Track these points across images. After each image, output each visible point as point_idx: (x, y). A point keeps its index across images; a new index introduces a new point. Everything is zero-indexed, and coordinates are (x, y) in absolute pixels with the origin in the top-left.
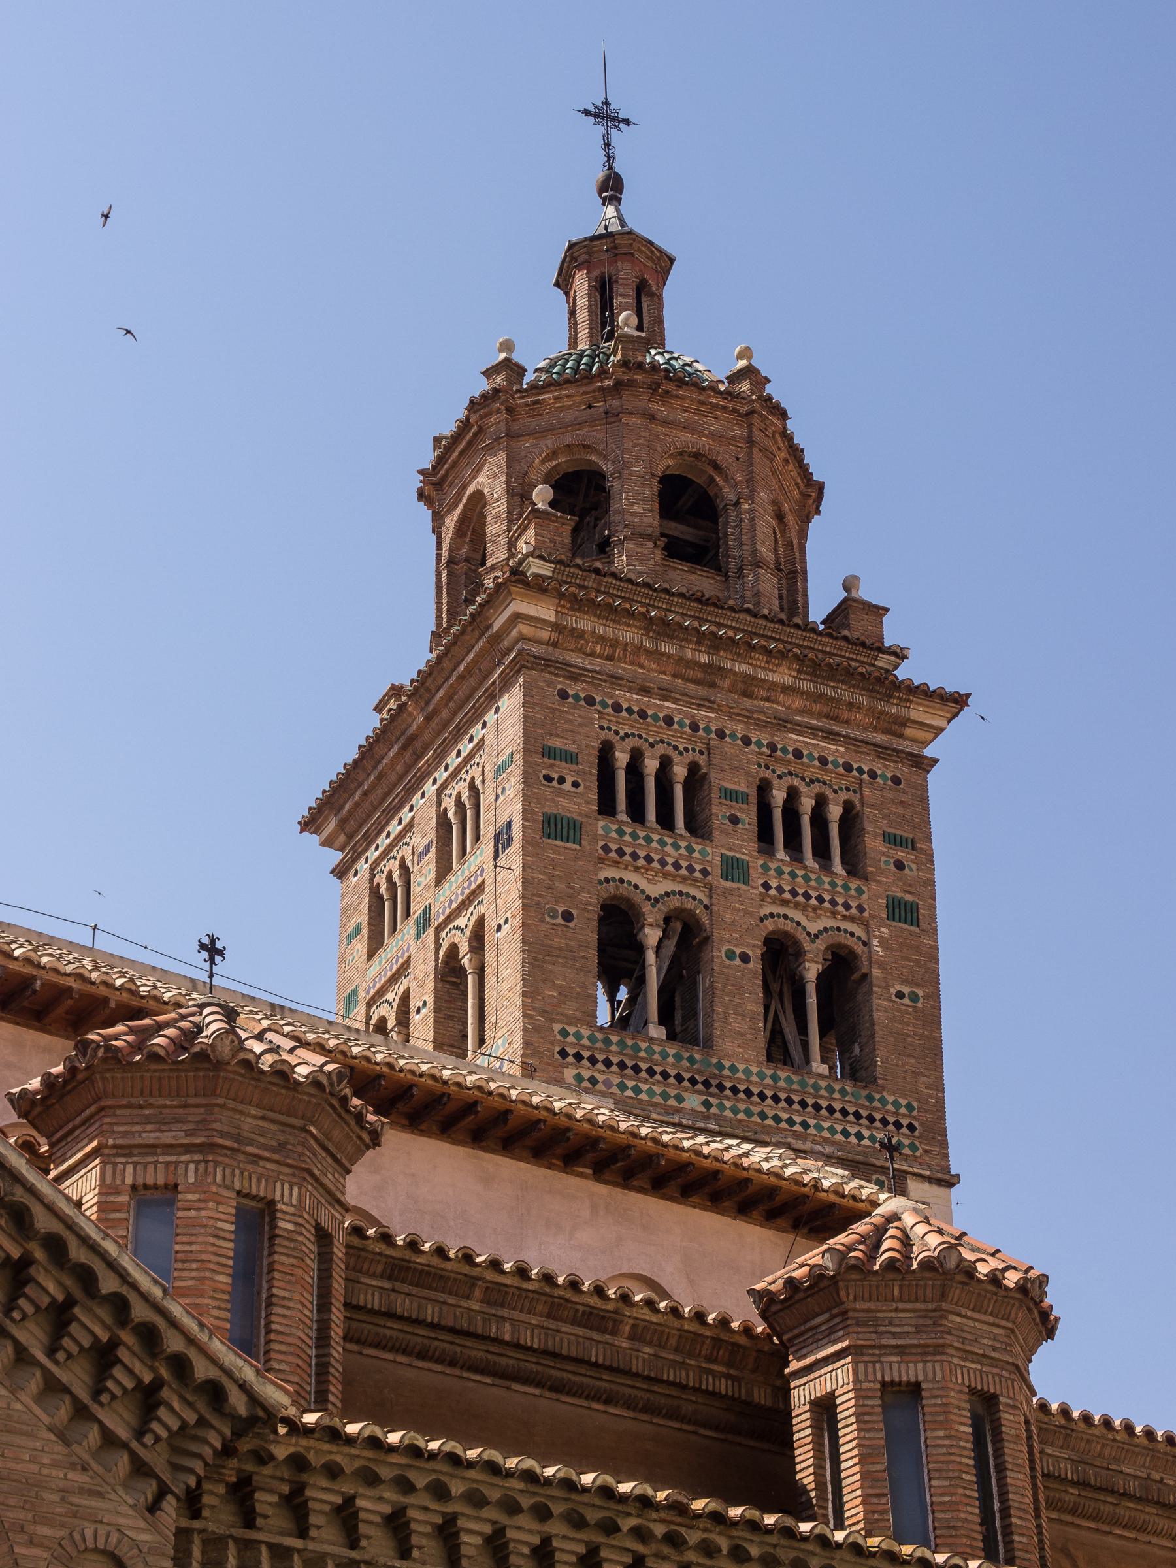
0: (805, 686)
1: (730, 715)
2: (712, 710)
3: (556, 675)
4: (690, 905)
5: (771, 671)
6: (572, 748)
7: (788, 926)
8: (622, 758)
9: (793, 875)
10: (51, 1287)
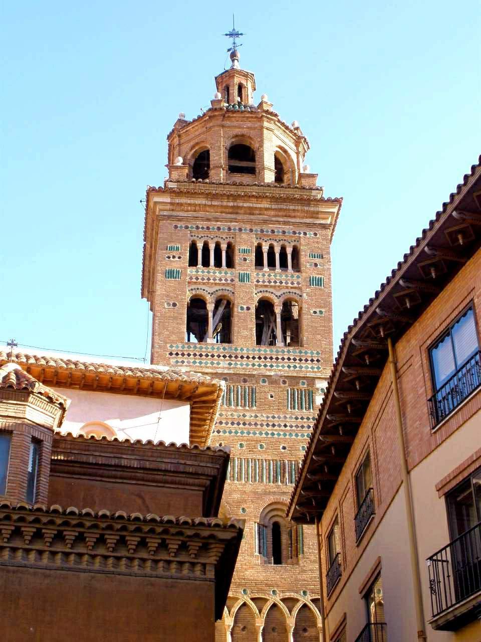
0: (274, 207)
1: (244, 222)
2: (237, 222)
3: (173, 221)
4: (226, 293)
5: (259, 204)
7: (267, 295)
9: (269, 275)
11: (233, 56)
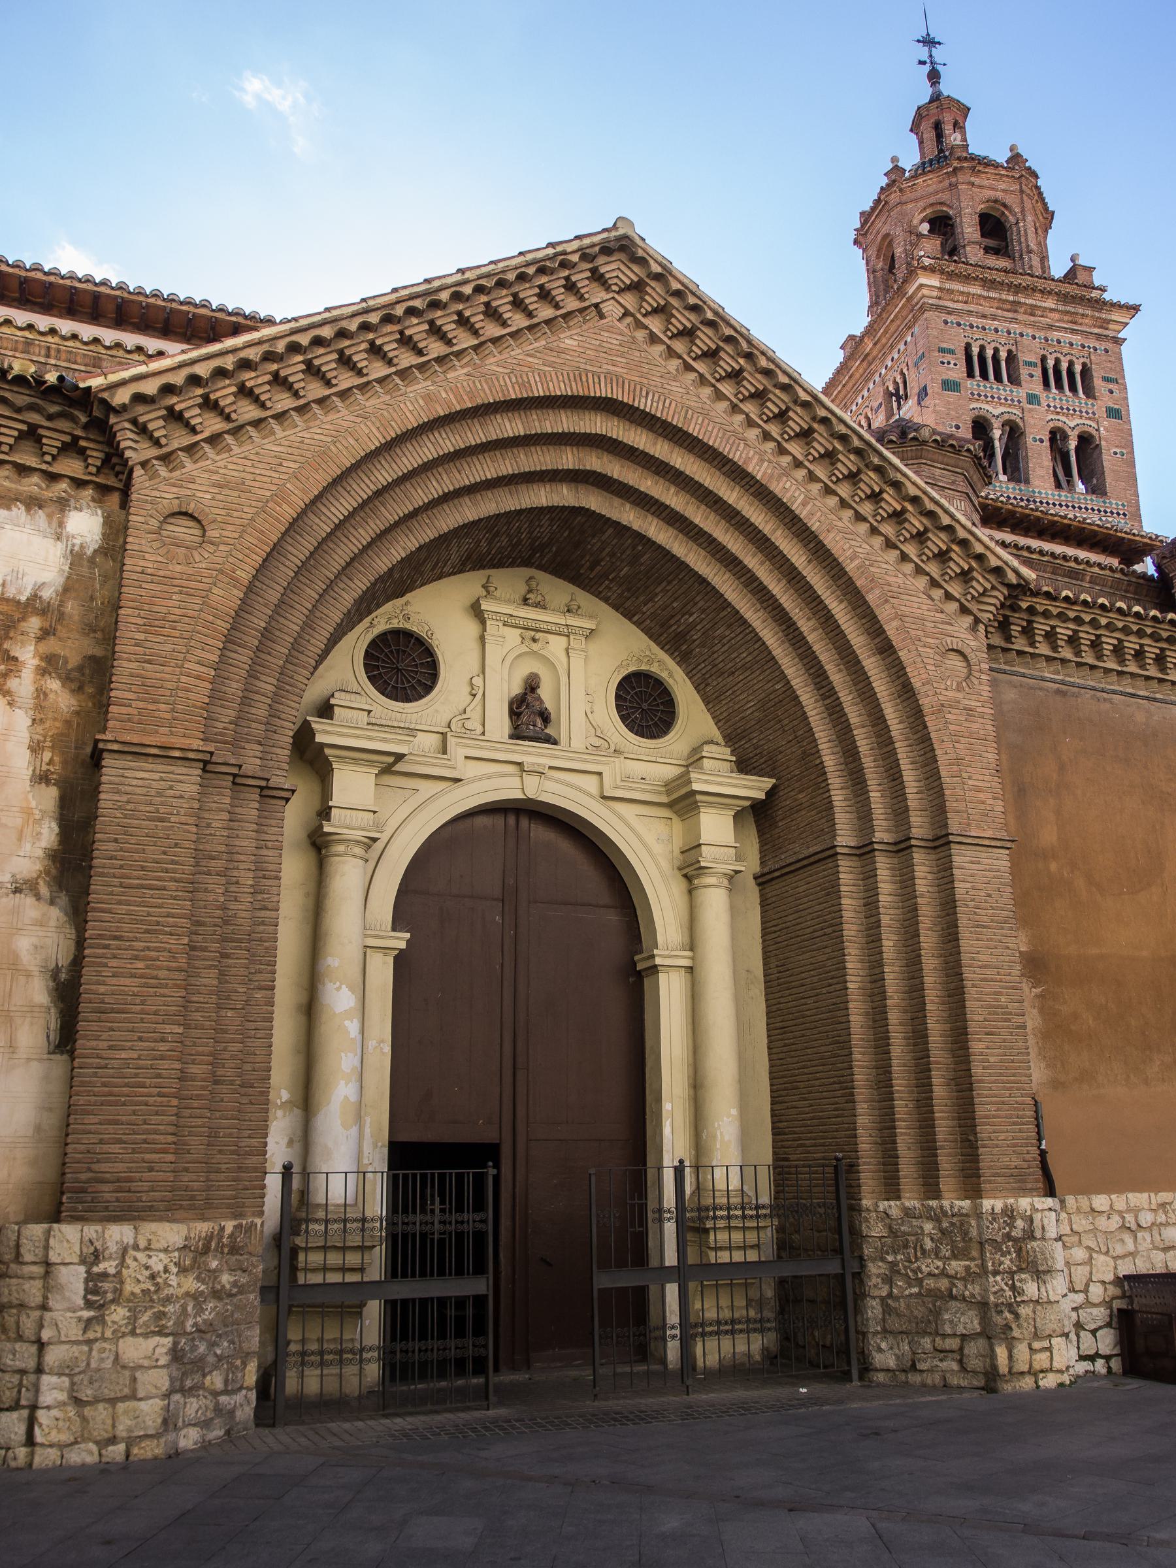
0: (1060, 308)
4: (1013, 417)
6: (952, 347)
7: (1060, 424)
8: (975, 350)
9: (1061, 400)
10: (917, 524)
11: (934, 77)
